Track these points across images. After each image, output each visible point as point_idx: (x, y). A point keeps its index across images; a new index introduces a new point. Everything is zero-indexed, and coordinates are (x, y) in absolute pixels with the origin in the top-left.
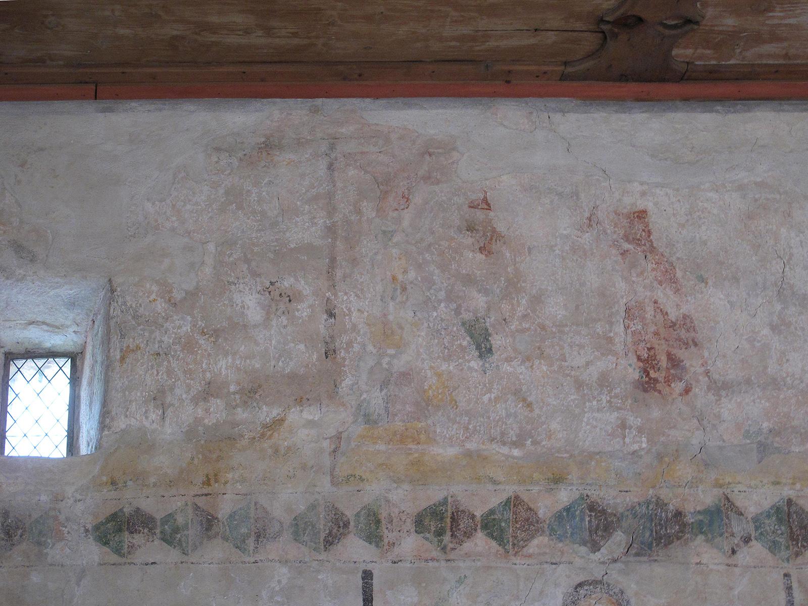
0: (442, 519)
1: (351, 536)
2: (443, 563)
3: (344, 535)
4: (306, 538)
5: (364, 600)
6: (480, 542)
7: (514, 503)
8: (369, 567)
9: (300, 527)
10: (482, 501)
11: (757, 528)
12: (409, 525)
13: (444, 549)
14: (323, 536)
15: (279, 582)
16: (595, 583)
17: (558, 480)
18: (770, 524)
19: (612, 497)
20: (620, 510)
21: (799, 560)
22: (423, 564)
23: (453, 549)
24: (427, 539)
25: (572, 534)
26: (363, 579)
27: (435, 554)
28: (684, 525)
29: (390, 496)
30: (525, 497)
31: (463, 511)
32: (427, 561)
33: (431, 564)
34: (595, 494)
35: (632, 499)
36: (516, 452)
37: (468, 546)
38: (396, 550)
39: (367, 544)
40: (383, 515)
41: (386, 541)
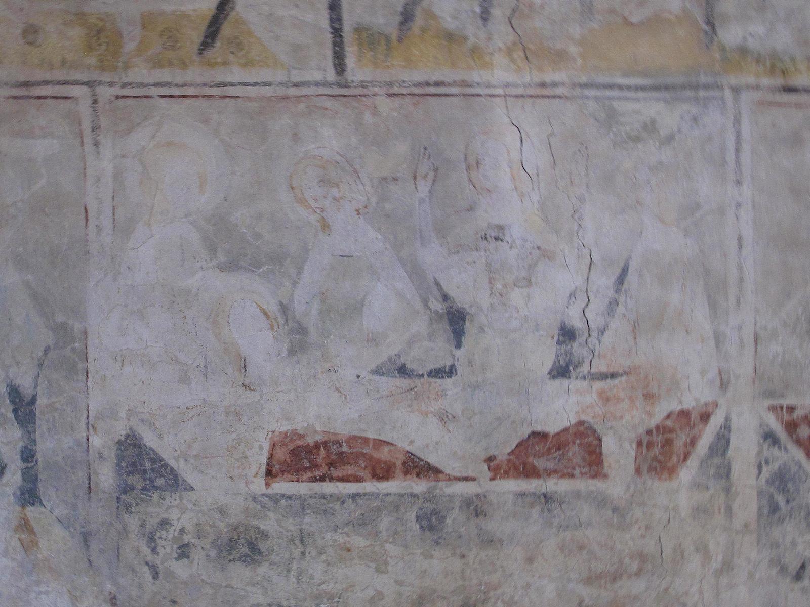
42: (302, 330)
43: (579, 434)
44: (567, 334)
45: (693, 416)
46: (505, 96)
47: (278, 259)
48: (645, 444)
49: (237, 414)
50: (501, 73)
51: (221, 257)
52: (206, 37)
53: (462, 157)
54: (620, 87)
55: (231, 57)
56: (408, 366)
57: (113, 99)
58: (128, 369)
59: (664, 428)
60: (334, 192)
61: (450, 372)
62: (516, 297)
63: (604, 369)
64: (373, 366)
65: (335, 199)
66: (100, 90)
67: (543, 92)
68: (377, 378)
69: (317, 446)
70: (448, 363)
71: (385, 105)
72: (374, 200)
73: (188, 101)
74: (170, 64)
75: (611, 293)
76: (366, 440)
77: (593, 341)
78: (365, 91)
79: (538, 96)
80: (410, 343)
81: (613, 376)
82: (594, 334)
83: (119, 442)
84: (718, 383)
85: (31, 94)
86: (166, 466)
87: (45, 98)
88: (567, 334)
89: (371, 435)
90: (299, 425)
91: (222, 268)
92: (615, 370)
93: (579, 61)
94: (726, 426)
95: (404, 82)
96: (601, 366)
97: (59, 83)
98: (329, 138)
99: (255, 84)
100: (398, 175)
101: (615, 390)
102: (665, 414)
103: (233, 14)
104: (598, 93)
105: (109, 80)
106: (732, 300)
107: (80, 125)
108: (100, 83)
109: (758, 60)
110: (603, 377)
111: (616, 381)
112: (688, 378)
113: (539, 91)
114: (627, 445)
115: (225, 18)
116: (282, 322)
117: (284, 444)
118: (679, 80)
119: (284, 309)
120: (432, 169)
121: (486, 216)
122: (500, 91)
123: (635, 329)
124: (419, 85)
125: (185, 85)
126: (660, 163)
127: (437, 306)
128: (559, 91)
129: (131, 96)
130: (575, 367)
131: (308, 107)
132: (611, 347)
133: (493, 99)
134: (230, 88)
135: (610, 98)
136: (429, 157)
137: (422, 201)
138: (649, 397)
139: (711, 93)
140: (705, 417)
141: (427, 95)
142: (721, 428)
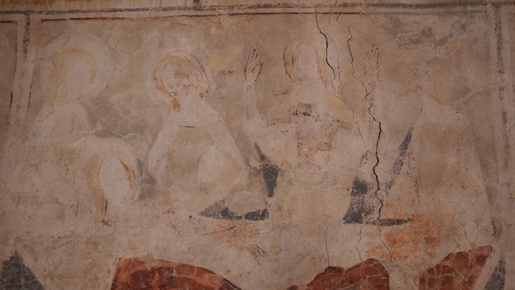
42: (152, 181)
43: (368, 270)
44: (360, 187)
45: (470, 259)
46: (316, 13)
47: (140, 129)
48: (427, 282)
49: (95, 244)
51: (100, 127)
53: (281, 56)
56: (230, 210)
57: (40, 22)
58: (21, 207)
59: (444, 267)
60: (186, 81)
61: (262, 215)
62: (319, 157)
63: (391, 216)
64: (203, 209)
65: (185, 86)
66: (32, 16)
68: (205, 218)
69: (153, 271)
70: (262, 209)
71: (227, 22)
72: (214, 87)
73: (89, 22)
75: (397, 155)
76: (192, 268)
77: (382, 193)
78: (213, 13)
79: (340, 13)
80: (233, 192)
81: (399, 222)
82: (382, 188)
83: (5, 263)
84: (491, 231)
86: (36, 282)
88: (360, 187)
89: (196, 264)
90: (141, 254)
91: (99, 135)
92: (401, 218)
94: (501, 269)
95: (242, 6)
96: (388, 214)
98: (185, 44)
99: (137, 10)
100: (233, 69)
101: (401, 235)
102: (445, 256)
104: (387, 10)
105: (39, 10)
106: (501, 163)
107: (16, 39)
110: (391, 222)
111: (402, 227)
112: (464, 226)
113: (342, 10)
114: (411, 281)
116: (137, 174)
117: (127, 269)
119: (140, 164)
120: (258, 64)
121: (298, 97)
122: (313, 10)
123: (417, 183)
124: (252, 7)
125: (88, 11)
126: (436, 59)
127: (257, 164)
128: (357, 9)
129: (51, 20)
130: (367, 214)
131: (171, 24)
132: (397, 197)
133: (307, 16)
134: (119, 12)
135: (399, 13)
136: (257, 56)
137: (249, 87)
138: (429, 240)
139: (477, 8)
140: (481, 260)
141: (258, 14)
142: (496, 269)
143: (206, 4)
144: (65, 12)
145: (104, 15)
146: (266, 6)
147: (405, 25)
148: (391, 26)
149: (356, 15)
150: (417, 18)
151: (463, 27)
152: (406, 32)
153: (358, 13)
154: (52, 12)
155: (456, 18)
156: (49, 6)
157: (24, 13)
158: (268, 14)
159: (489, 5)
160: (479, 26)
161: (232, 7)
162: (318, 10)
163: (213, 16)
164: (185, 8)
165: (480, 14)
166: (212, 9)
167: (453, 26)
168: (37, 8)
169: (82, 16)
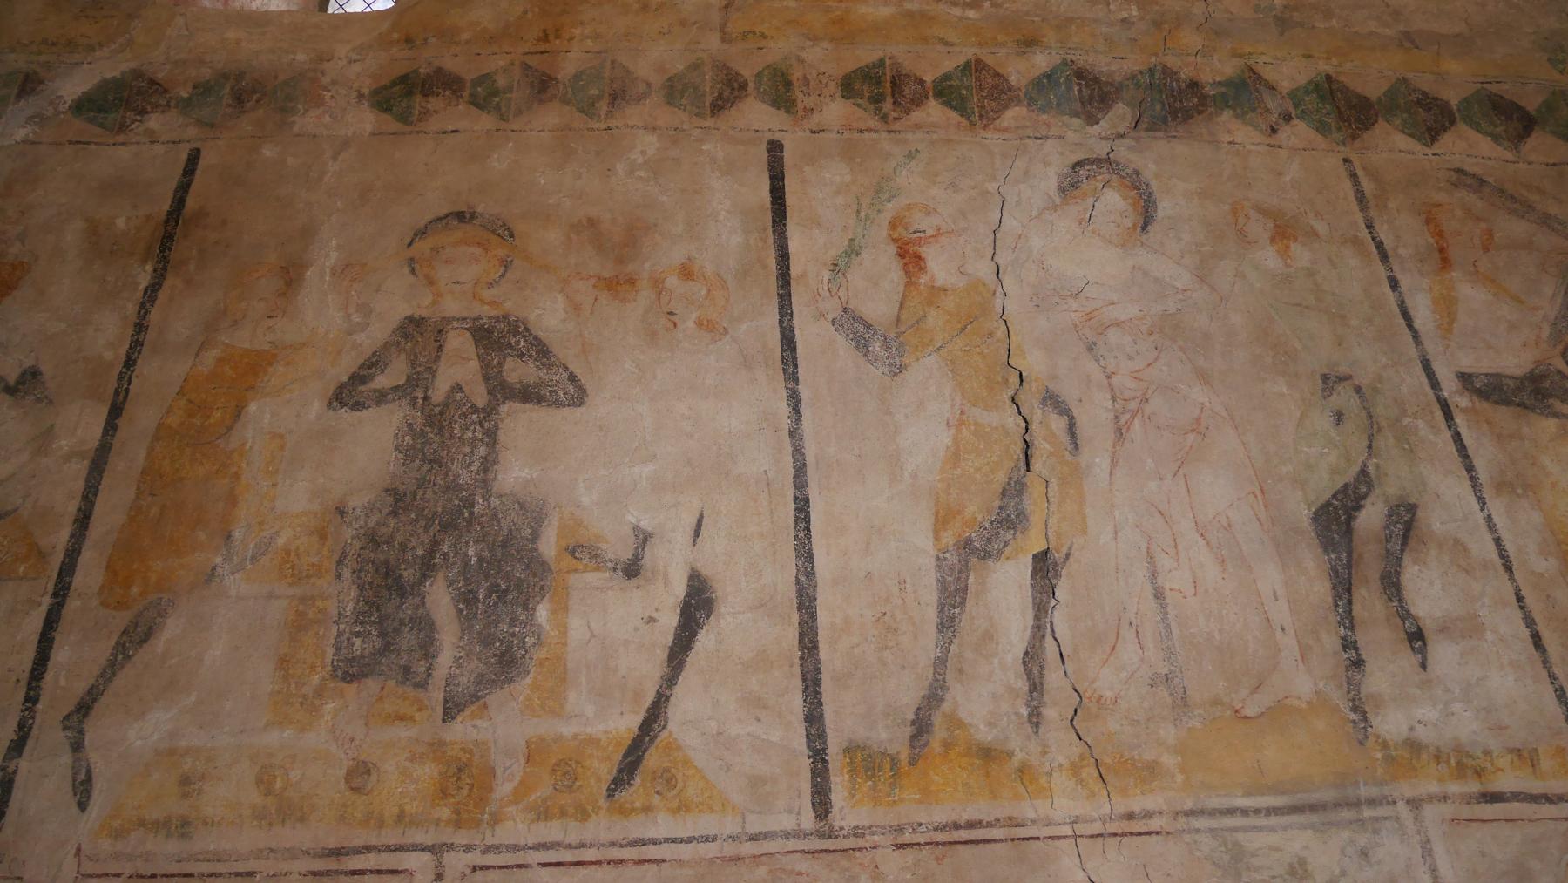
0: (878, 83)
1: (750, 100)
2: (884, 135)
3: (740, 98)
4: (684, 102)
5: (771, 178)
6: (934, 111)
7: (975, 67)
8: (777, 137)
9: (674, 90)
10: (932, 66)
11: (1296, 106)
12: (832, 87)
13: (884, 118)
14: (709, 99)
15: (643, 153)
16: (1098, 161)
17: (1030, 43)
18: (1311, 101)
19: (1103, 63)
20: (1118, 79)
21: (1357, 143)
22: (856, 135)
23: (896, 119)
24: (859, 106)
25: (1059, 105)
26: (769, 151)
27: (873, 122)
28: (1203, 98)
29: (804, 55)
30: (989, 60)
31: (907, 76)
32: (861, 131)
33: (866, 135)
34: (1082, 59)
35: (1133, 63)
36: (971, 14)
37: (917, 115)
38: (816, 119)
39: (773, 110)
40: (796, 75)
41: (800, 106)
50: (1065, 802)
52: (620, 771)
54: (1245, 812)
55: (656, 800)
67: (1131, 828)
74: (563, 813)
78: (860, 843)
79: (1123, 835)
85: (342, 867)
87: (362, 872)
93: (1179, 778)
97: (388, 849)
103: (664, 734)
108: (451, 847)
109: (1438, 757)
115: (652, 740)
118: (1328, 795)
128: (1155, 824)
133: (1057, 843)
135: (1236, 830)
143: (843, 823)
144: (526, 848)
145: (616, 854)
146: (971, 825)
147: (1253, 855)
148: (1226, 858)
149: (1154, 838)
150: (1273, 839)
151: (1364, 854)
152: (1257, 869)
153: (1158, 833)
154: (497, 848)
155: (1346, 834)
156: (488, 834)
157: (430, 849)
158: (977, 842)
159: (1401, 805)
160: (1393, 849)
161: (900, 829)
162: (1081, 829)
163: (860, 849)
164: (799, 834)
165: (1388, 824)
166: (855, 835)
167: (1343, 852)
168: (461, 838)
169: (568, 856)
